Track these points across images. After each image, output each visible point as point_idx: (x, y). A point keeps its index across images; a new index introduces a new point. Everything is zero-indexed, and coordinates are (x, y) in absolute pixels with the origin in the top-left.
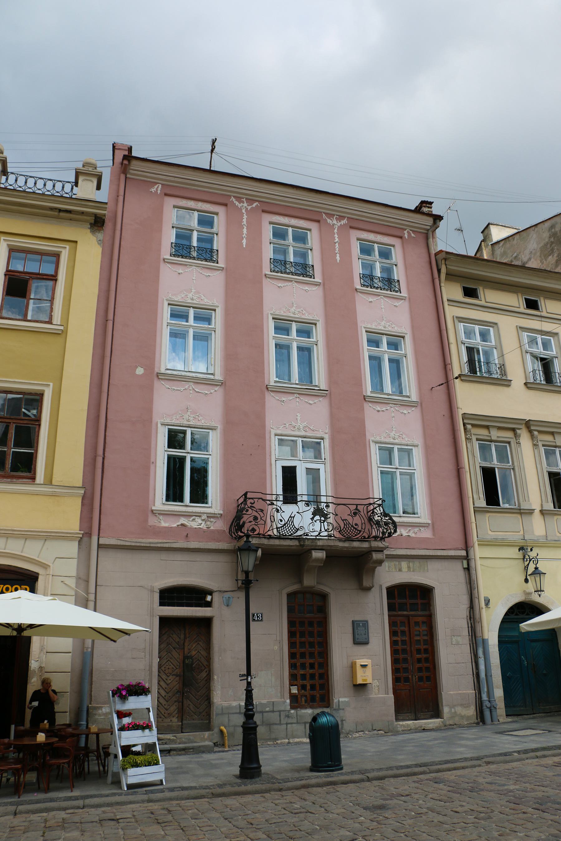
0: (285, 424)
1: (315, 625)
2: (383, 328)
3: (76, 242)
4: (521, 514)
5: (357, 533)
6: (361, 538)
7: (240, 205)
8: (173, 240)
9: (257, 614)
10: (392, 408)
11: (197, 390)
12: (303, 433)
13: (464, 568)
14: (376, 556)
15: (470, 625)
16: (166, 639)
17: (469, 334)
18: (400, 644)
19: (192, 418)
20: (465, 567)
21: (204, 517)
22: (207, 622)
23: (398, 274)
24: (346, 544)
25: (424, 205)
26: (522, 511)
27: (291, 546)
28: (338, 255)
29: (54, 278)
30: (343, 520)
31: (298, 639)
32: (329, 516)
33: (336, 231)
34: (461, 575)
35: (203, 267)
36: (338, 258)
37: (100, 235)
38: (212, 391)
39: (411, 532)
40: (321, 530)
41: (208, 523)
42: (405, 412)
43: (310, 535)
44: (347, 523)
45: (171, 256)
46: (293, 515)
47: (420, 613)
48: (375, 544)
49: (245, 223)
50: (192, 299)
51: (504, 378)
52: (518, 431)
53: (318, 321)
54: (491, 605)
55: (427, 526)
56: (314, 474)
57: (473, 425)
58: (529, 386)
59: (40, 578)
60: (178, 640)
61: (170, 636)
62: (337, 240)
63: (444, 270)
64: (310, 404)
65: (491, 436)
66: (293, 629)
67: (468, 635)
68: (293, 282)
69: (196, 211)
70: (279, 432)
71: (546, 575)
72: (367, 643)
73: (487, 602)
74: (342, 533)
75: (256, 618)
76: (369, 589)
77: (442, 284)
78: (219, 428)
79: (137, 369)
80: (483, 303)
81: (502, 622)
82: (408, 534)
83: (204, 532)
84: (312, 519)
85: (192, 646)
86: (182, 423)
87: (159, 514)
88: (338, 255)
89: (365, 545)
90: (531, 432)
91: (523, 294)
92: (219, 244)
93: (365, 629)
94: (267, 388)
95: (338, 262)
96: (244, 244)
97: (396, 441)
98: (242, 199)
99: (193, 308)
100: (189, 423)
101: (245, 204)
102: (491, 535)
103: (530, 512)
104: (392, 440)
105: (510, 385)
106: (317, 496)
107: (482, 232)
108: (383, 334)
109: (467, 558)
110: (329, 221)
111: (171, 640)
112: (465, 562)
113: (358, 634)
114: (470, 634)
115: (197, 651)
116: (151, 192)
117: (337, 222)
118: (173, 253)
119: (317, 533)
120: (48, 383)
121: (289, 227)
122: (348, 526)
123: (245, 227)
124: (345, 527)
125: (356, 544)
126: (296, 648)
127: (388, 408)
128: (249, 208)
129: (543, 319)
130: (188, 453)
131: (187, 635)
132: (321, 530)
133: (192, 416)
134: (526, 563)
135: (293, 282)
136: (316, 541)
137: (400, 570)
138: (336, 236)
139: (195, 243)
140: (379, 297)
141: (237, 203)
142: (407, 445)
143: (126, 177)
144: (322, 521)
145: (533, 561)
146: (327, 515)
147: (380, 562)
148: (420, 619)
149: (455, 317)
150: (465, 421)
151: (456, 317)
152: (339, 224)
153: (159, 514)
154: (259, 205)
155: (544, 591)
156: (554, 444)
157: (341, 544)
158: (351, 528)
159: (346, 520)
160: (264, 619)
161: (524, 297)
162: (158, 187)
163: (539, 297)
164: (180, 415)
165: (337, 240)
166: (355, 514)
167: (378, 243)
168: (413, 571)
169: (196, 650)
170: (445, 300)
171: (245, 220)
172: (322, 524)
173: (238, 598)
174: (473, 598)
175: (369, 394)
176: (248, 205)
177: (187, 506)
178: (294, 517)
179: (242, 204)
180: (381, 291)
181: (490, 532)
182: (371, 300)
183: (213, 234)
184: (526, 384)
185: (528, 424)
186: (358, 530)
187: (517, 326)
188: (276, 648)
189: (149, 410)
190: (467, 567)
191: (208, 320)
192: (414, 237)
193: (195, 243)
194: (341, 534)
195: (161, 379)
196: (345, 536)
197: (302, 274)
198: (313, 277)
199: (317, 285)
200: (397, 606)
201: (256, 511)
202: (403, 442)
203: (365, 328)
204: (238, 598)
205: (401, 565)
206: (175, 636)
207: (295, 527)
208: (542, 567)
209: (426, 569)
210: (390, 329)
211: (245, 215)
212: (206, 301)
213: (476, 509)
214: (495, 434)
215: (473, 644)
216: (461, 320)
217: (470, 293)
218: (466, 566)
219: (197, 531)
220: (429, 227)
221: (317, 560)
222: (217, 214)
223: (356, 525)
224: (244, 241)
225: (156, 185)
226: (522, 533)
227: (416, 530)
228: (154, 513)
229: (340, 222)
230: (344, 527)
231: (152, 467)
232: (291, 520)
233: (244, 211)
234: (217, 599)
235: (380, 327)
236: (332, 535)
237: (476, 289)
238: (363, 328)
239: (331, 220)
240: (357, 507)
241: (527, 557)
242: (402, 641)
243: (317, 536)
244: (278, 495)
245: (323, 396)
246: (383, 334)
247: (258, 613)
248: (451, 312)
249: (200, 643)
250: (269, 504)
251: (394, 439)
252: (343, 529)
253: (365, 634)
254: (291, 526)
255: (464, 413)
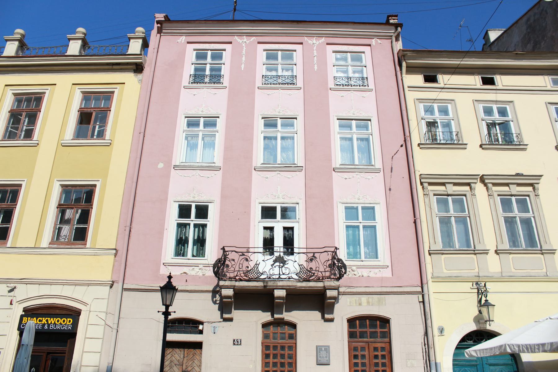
0: (268, 195)
1: (286, 349)
2: (352, 115)
3: (124, 83)
4: (475, 254)
5: (311, 275)
6: (317, 279)
7: (241, 41)
8: (192, 72)
9: (237, 340)
10: (358, 175)
11: (202, 175)
12: (281, 200)
13: (420, 302)
14: (329, 293)
15: (424, 351)
16: (170, 358)
17: (429, 110)
18: (360, 365)
19: (197, 196)
20: (420, 301)
21: (201, 266)
22: (198, 345)
23: (368, 73)
24: (304, 284)
25: (390, 18)
26: (476, 252)
27: (257, 287)
28: (316, 65)
29: (108, 109)
30: (299, 265)
31: (271, 360)
32: (287, 262)
33: (315, 48)
34: (418, 308)
35: (212, 88)
36: (316, 68)
37: (140, 76)
38: (213, 175)
39: (372, 273)
40: (280, 274)
41: (204, 271)
42: (369, 177)
43: (272, 278)
44: (302, 267)
45: (189, 84)
46: (258, 263)
47: (379, 340)
48: (328, 283)
49: (244, 53)
50: (202, 111)
51: (460, 142)
52: (472, 185)
53: (298, 115)
54: (445, 333)
55: (386, 268)
56: (289, 230)
57: (430, 184)
58: (484, 146)
59: (83, 313)
60: (178, 358)
61: (173, 356)
62: (315, 54)
63: (404, 64)
64: (289, 178)
65: (447, 191)
66: (268, 352)
67: (423, 359)
68: (280, 90)
69: (210, 51)
70: (262, 201)
71: (495, 307)
72: (329, 365)
73: (441, 330)
74: (299, 275)
75: (236, 343)
76: (332, 320)
77: (403, 76)
78: (216, 201)
79: (159, 164)
80: (442, 85)
81: (457, 348)
82: (368, 275)
83: (200, 278)
84: (272, 265)
85: (189, 363)
86: (188, 199)
87: (168, 265)
88: (316, 65)
89: (320, 284)
90: (485, 185)
91: (479, 74)
92: (225, 71)
93: (327, 353)
94: (255, 169)
95: (316, 70)
96: (243, 68)
97: (361, 201)
98: (243, 37)
99: (203, 117)
100: (194, 199)
101: (245, 40)
102: (446, 272)
103: (485, 252)
104: (357, 201)
105: (466, 148)
106: (280, 247)
107: (484, 38)
108: (352, 120)
109: (422, 293)
110: (310, 42)
111: (174, 358)
112: (421, 296)
113: (320, 357)
114: (425, 358)
115: (192, 367)
116: (178, 42)
117: (316, 42)
118: (192, 82)
119: (277, 277)
120: (99, 180)
121: (278, 51)
122: (303, 270)
123: (244, 56)
124: (301, 271)
125: (312, 284)
126: (269, 367)
127: (355, 176)
128: (248, 42)
129: (498, 91)
130: (192, 221)
131: (186, 355)
132: (280, 274)
133: (197, 194)
134: (480, 296)
135: (280, 90)
136: (277, 283)
137: (360, 304)
138: (315, 52)
139: (208, 72)
140: (350, 92)
141: (239, 40)
142: (370, 204)
143: (161, 36)
144: (281, 267)
145: (484, 294)
146: (286, 261)
147: (336, 299)
148: (379, 345)
149: (415, 100)
150: (422, 180)
151: (417, 99)
152: (318, 43)
153: (168, 265)
154: (255, 39)
155: (493, 321)
156: (510, 193)
157: (299, 284)
158: (306, 271)
159: (302, 265)
160: (242, 344)
161: (480, 76)
162: (182, 39)
163: (495, 74)
164: (188, 194)
165: (315, 54)
166: (311, 260)
167: (350, 52)
168: (372, 305)
169: (192, 366)
170: (406, 87)
171: (244, 52)
172: (281, 269)
173: (223, 327)
174: (427, 327)
175: (338, 166)
176: (247, 40)
177: (189, 259)
178: (259, 264)
179: (242, 40)
180: (351, 87)
181: (445, 271)
182: (342, 95)
183: (221, 64)
184: (481, 146)
185: (482, 179)
186: (312, 273)
187: (473, 100)
188: (251, 366)
189: (166, 193)
190: (422, 301)
191: (214, 125)
192: (380, 43)
193: (208, 72)
194: (298, 276)
195: (176, 170)
196: (301, 278)
197: (287, 83)
198: (295, 84)
199: (299, 89)
200: (358, 334)
201: (229, 261)
202: (367, 201)
203: (336, 116)
204: (223, 327)
205: (361, 300)
206: (176, 355)
207: (259, 272)
208: (491, 298)
209: (384, 303)
210: (358, 115)
211: (244, 47)
212: (213, 113)
213: (430, 252)
214: (451, 189)
215: (427, 367)
216: (421, 100)
217: (430, 79)
218: (421, 300)
219: (194, 277)
220: (392, 34)
221: (279, 298)
222: (225, 50)
223: (311, 268)
224: (243, 66)
225: (181, 37)
226: (477, 270)
227: (377, 270)
228: (165, 265)
229: (318, 41)
230: (300, 271)
231: (165, 231)
232: (256, 266)
233: (244, 45)
234: (206, 328)
235: (349, 115)
236: (291, 278)
237: (436, 76)
238: (334, 116)
239: (312, 41)
240: (314, 254)
241: (480, 291)
242: (362, 363)
243: (278, 278)
244: (249, 248)
245: (299, 171)
246: (352, 120)
247: (237, 339)
248: (411, 96)
249: (195, 361)
250: (241, 255)
251: (359, 199)
252: (299, 273)
253: (326, 357)
254: (256, 271)
255: (421, 175)
